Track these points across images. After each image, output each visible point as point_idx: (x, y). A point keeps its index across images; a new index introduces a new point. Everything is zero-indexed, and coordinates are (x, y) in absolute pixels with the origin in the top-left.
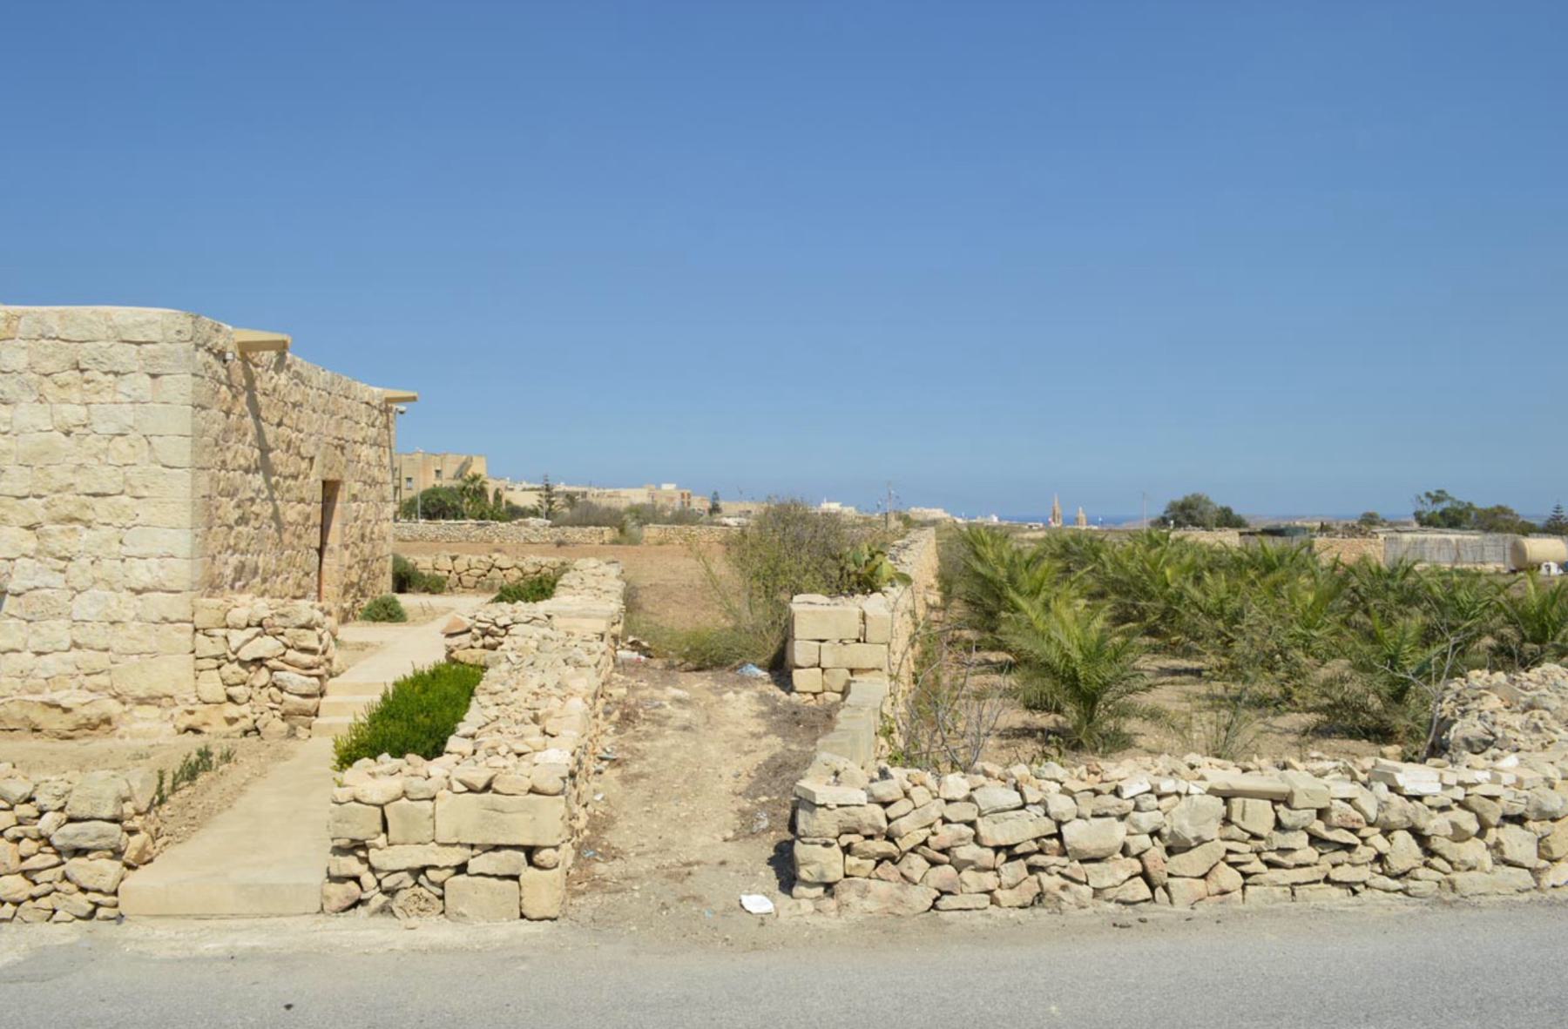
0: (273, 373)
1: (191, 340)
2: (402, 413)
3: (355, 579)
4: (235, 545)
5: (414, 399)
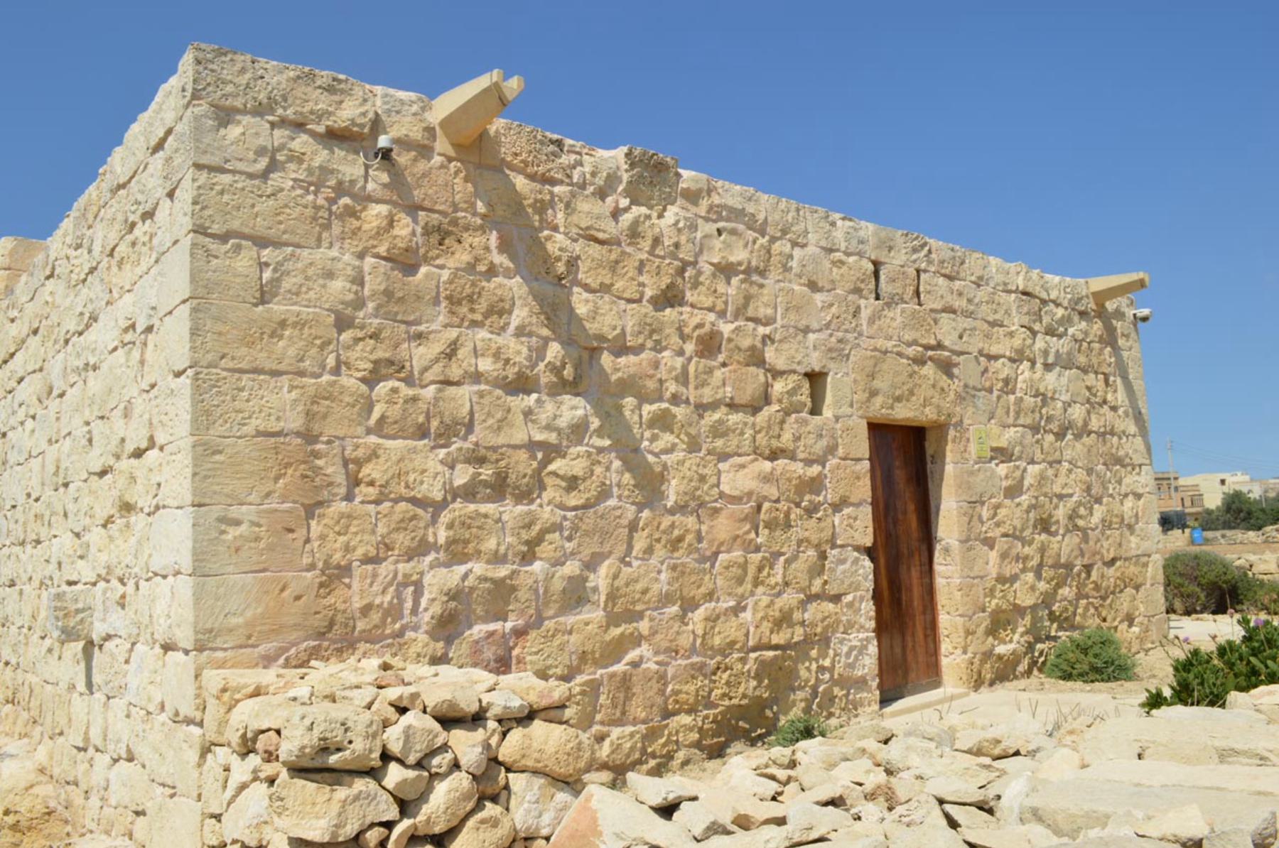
0: (624, 202)
1: (196, 95)
2: (1145, 319)
3: (1027, 600)
4: (451, 542)
5: (1141, 284)
